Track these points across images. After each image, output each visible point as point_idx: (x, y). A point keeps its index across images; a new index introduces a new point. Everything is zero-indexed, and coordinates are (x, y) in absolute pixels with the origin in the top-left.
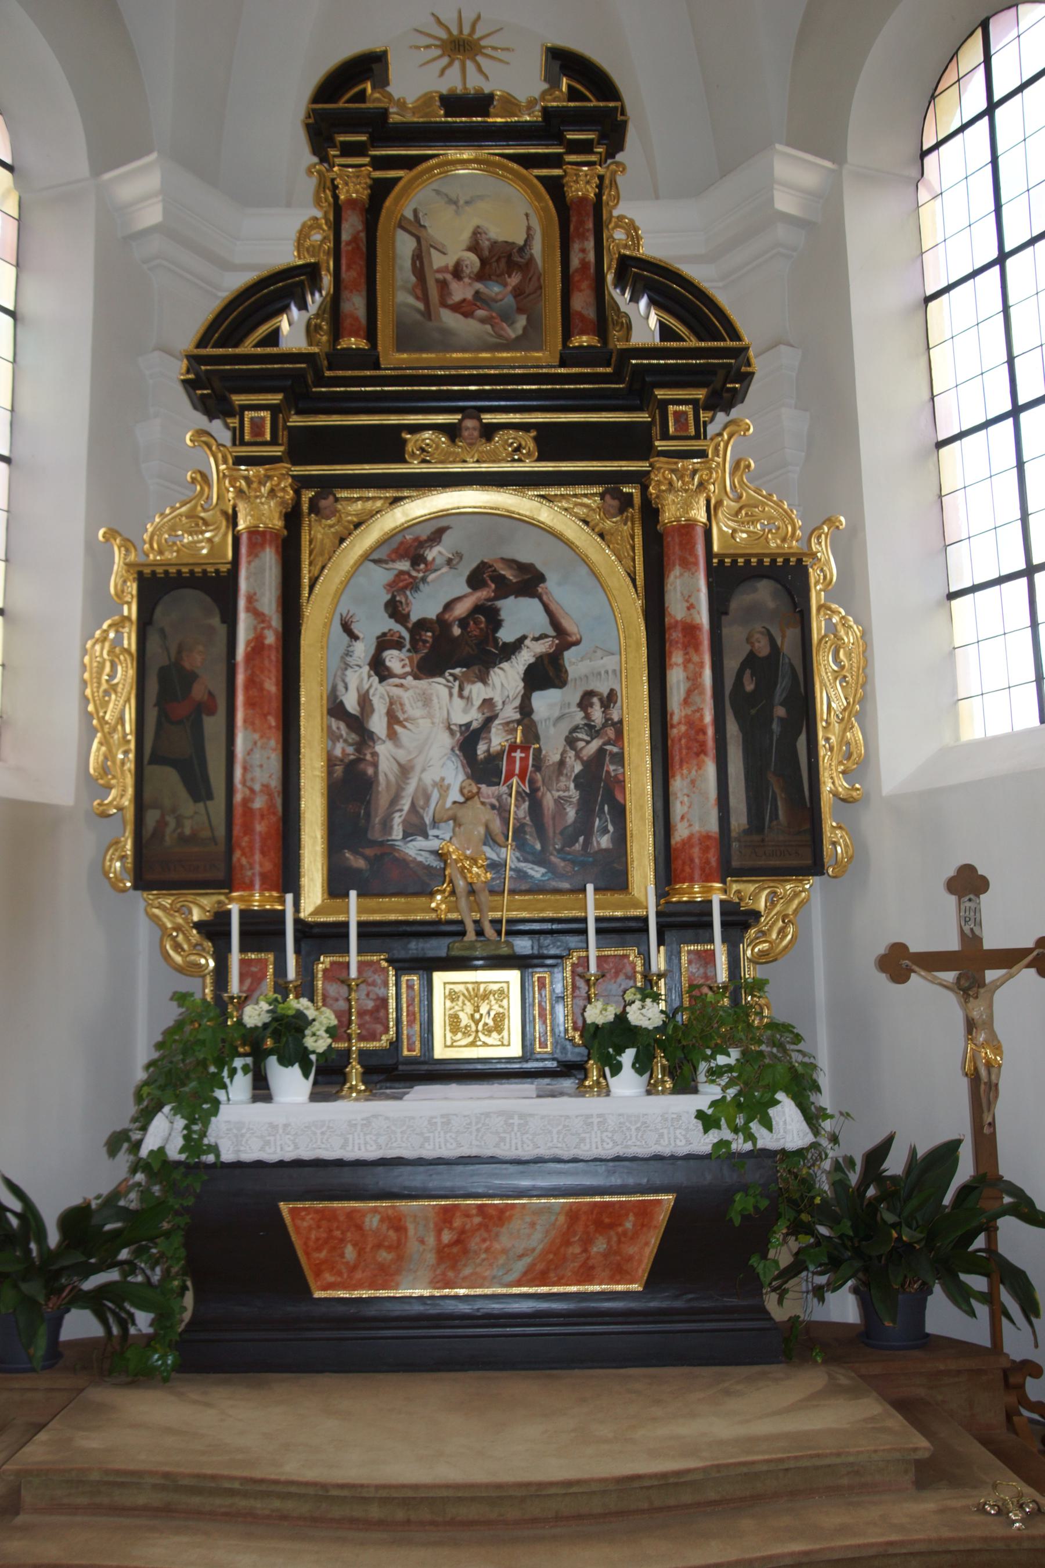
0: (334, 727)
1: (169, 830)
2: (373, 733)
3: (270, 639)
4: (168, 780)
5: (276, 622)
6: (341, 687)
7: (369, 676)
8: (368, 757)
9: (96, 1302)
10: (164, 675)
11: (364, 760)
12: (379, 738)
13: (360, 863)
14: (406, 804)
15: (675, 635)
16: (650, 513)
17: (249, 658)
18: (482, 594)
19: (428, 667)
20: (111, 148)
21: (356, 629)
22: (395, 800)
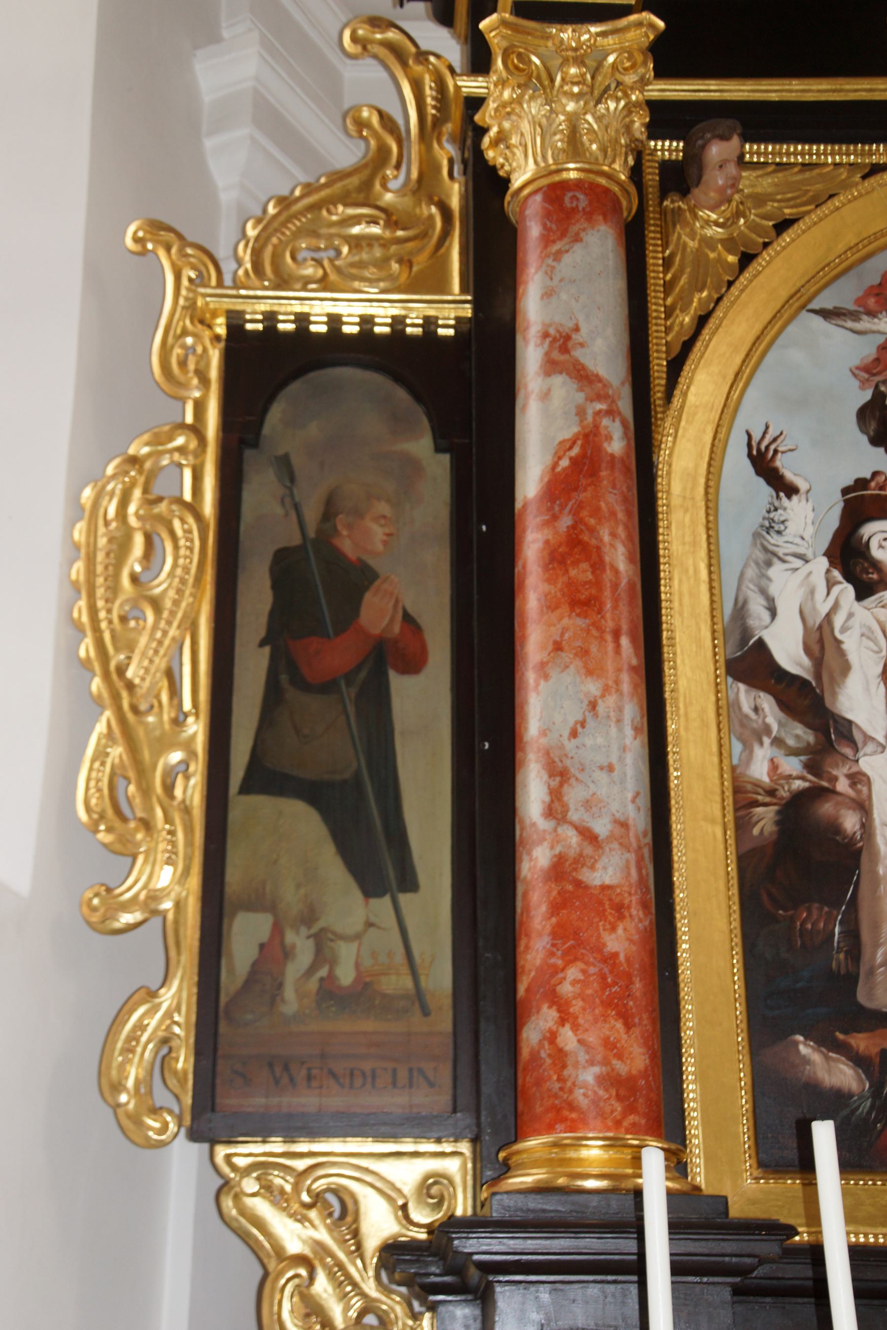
0: (747, 708)
1: (293, 971)
2: (850, 722)
4: (290, 836)
5: (625, 406)
6: (757, 607)
7: (830, 584)
8: (843, 785)
10: (286, 568)
11: (833, 792)
12: (868, 738)
13: (842, 1075)
17: (559, 488)
21: (786, 466)
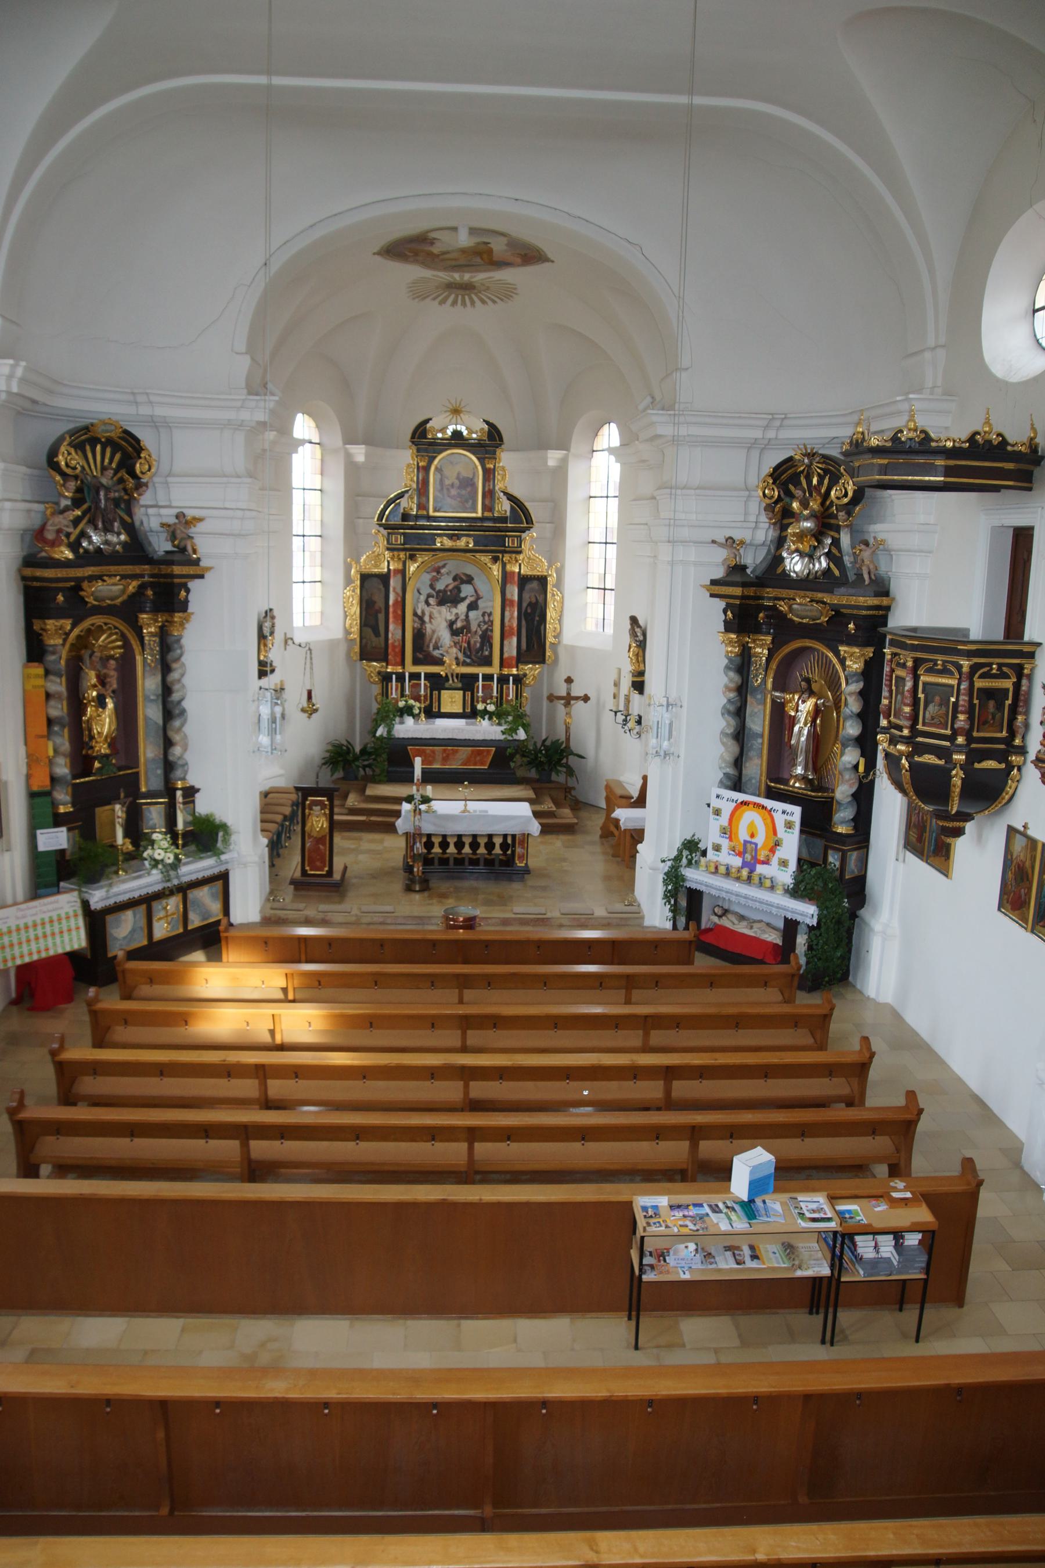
3: (399, 599)
4: (369, 631)
9: (364, 767)
14: (434, 641)
16: (504, 565)
17: (394, 605)
19: (441, 603)
20: (350, 439)
22: (431, 640)
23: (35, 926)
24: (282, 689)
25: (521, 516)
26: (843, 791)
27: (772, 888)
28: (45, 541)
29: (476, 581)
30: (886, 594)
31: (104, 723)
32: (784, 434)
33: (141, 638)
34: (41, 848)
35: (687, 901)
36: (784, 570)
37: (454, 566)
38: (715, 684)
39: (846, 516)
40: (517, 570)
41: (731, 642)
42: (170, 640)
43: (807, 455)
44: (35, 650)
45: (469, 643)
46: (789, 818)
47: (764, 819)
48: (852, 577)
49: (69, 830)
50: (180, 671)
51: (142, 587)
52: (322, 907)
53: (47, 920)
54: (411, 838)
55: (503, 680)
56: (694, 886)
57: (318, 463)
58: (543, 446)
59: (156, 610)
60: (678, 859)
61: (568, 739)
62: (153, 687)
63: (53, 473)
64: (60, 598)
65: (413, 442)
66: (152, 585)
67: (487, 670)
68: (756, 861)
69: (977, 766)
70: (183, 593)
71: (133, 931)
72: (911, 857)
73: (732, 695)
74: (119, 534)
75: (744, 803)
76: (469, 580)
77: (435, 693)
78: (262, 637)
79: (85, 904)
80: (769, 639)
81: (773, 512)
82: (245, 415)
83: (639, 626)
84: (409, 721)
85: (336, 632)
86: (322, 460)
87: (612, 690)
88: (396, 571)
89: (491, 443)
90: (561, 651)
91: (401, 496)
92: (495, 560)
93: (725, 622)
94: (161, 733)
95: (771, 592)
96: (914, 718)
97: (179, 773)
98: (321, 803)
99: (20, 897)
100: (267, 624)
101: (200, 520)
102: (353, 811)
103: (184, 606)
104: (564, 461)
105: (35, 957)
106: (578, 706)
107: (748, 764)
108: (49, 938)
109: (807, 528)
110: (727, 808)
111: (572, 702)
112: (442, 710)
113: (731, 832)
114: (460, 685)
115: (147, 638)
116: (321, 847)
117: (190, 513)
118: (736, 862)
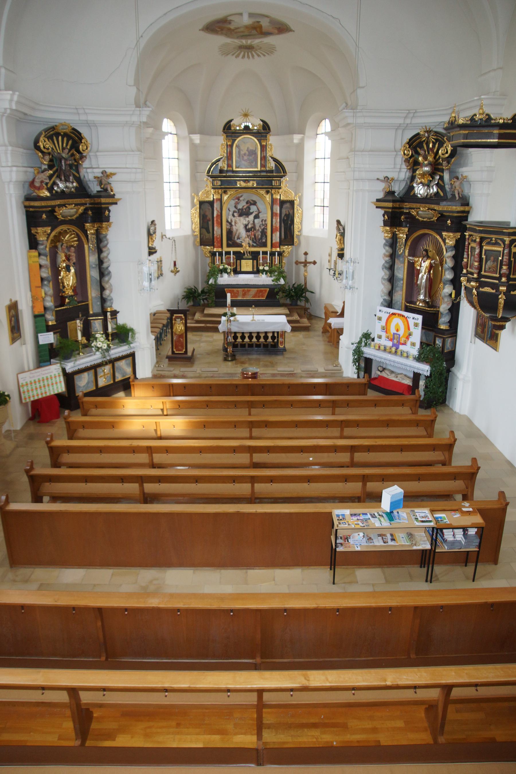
3: (219, 214)
4: (204, 231)
5: (220, 211)
9: (203, 300)
15: (274, 214)
16: (272, 195)
18: (248, 205)
19: (240, 215)
20: (192, 132)
22: (235, 234)
23: (39, 381)
24: (161, 261)
25: (280, 169)
26: (444, 307)
27: (407, 357)
28: (35, 187)
29: (258, 204)
30: (468, 204)
31: (69, 279)
32: (415, 121)
33: (87, 236)
34: (41, 343)
35: (365, 364)
36: (414, 193)
37: (246, 196)
38: (379, 253)
39: (447, 164)
40: (279, 198)
41: (387, 231)
42: (102, 236)
43: (427, 132)
44: (33, 243)
45: (255, 236)
46: (416, 321)
47: (403, 322)
48: (449, 196)
49: (54, 333)
50: (107, 252)
51: (86, 210)
52: (183, 369)
53: (45, 378)
54: (226, 334)
55: (272, 254)
56: (368, 356)
57: (176, 145)
58: (291, 132)
59: (94, 221)
60: (360, 342)
61: (306, 284)
62: (94, 261)
63: (37, 152)
64: (44, 216)
65: (224, 132)
66: (91, 209)
67: (264, 249)
68: (399, 343)
69: (512, 293)
70: (107, 212)
71: (88, 383)
72: (478, 341)
73: (387, 259)
74: (73, 183)
75: (394, 314)
76: (255, 203)
77: (238, 261)
78: (150, 235)
79: (64, 370)
80: (406, 229)
81: (409, 163)
82: (135, 119)
83: (341, 225)
84: (225, 275)
85: (188, 231)
86: (178, 143)
87: (328, 258)
88: (217, 199)
89: (264, 131)
90: (302, 239)
91: (218, 160)
92: (267, 192)
93: (384, 221)
94: (99, 284)
95: (407, 205)
96: (480, 268)
97: (108, 304)
98: (180, 317)
99: (32, 367)
100: (152, 228)
101: (114, 174)
102: (198, 322)
103: (107, 219)
104: (302, 141)
105: (40, 397)
106: (311, 267)
107: (395, 294)
108: (47, 387)
109: (426, 171)
110: (385, 317)
111: (308, 265)
112: (242, 270)
113: (387, 329)
114: (251, 257)
115: (90, 236)
116: (181, 339)
117: (109, 171)
118: (389, 344)
